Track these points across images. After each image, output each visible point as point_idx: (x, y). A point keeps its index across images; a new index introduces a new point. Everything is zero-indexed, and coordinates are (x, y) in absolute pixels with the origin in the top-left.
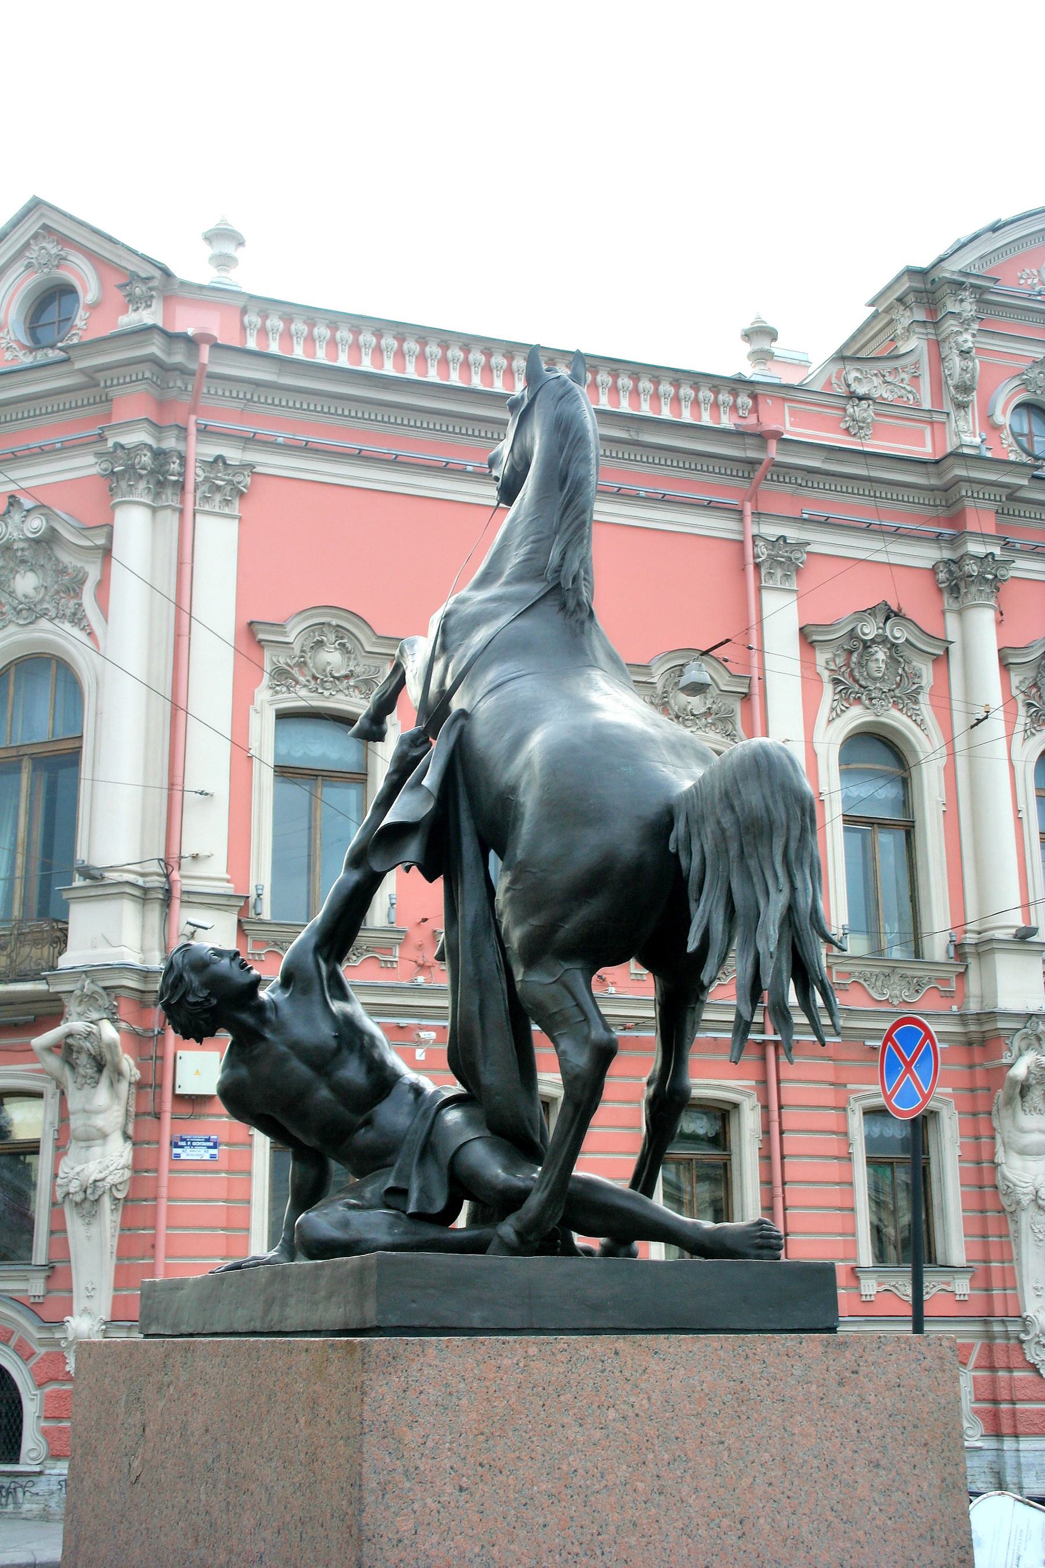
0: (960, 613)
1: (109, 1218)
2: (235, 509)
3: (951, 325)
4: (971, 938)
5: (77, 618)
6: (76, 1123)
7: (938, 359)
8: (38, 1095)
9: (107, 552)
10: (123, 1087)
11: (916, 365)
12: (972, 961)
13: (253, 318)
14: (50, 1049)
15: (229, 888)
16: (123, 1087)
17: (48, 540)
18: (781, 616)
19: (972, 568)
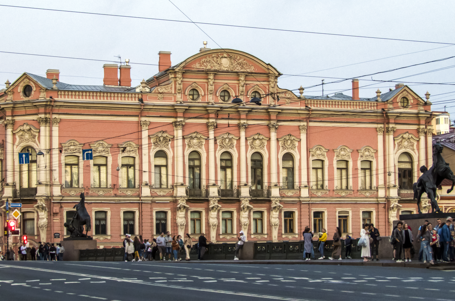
0: (177, 130)
1: (45, 230)
2: (58, 125)
3: (178, 79)
4: (175, 185)
5: (35, 142)
6: (40, 217)
7: (175, 84)
8: (34, 212)
9: (39, 132)
10: (46, 212)
11: (172, 85)
12: (175, 188)
13: (59, 93)
14: (36, 207)
15: (59, 183)
16: (46, 212)
17: (30, 130)
18: (145, 134)
19: (178, 123)
